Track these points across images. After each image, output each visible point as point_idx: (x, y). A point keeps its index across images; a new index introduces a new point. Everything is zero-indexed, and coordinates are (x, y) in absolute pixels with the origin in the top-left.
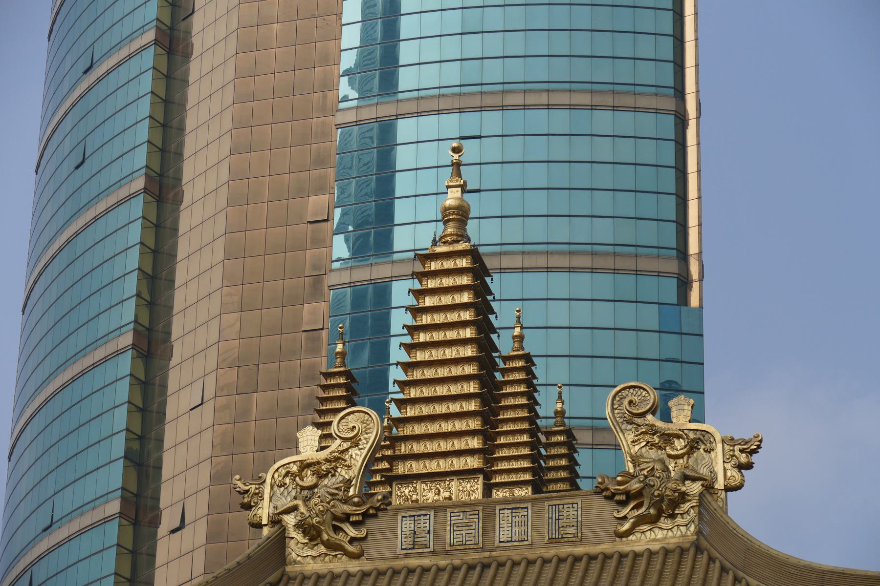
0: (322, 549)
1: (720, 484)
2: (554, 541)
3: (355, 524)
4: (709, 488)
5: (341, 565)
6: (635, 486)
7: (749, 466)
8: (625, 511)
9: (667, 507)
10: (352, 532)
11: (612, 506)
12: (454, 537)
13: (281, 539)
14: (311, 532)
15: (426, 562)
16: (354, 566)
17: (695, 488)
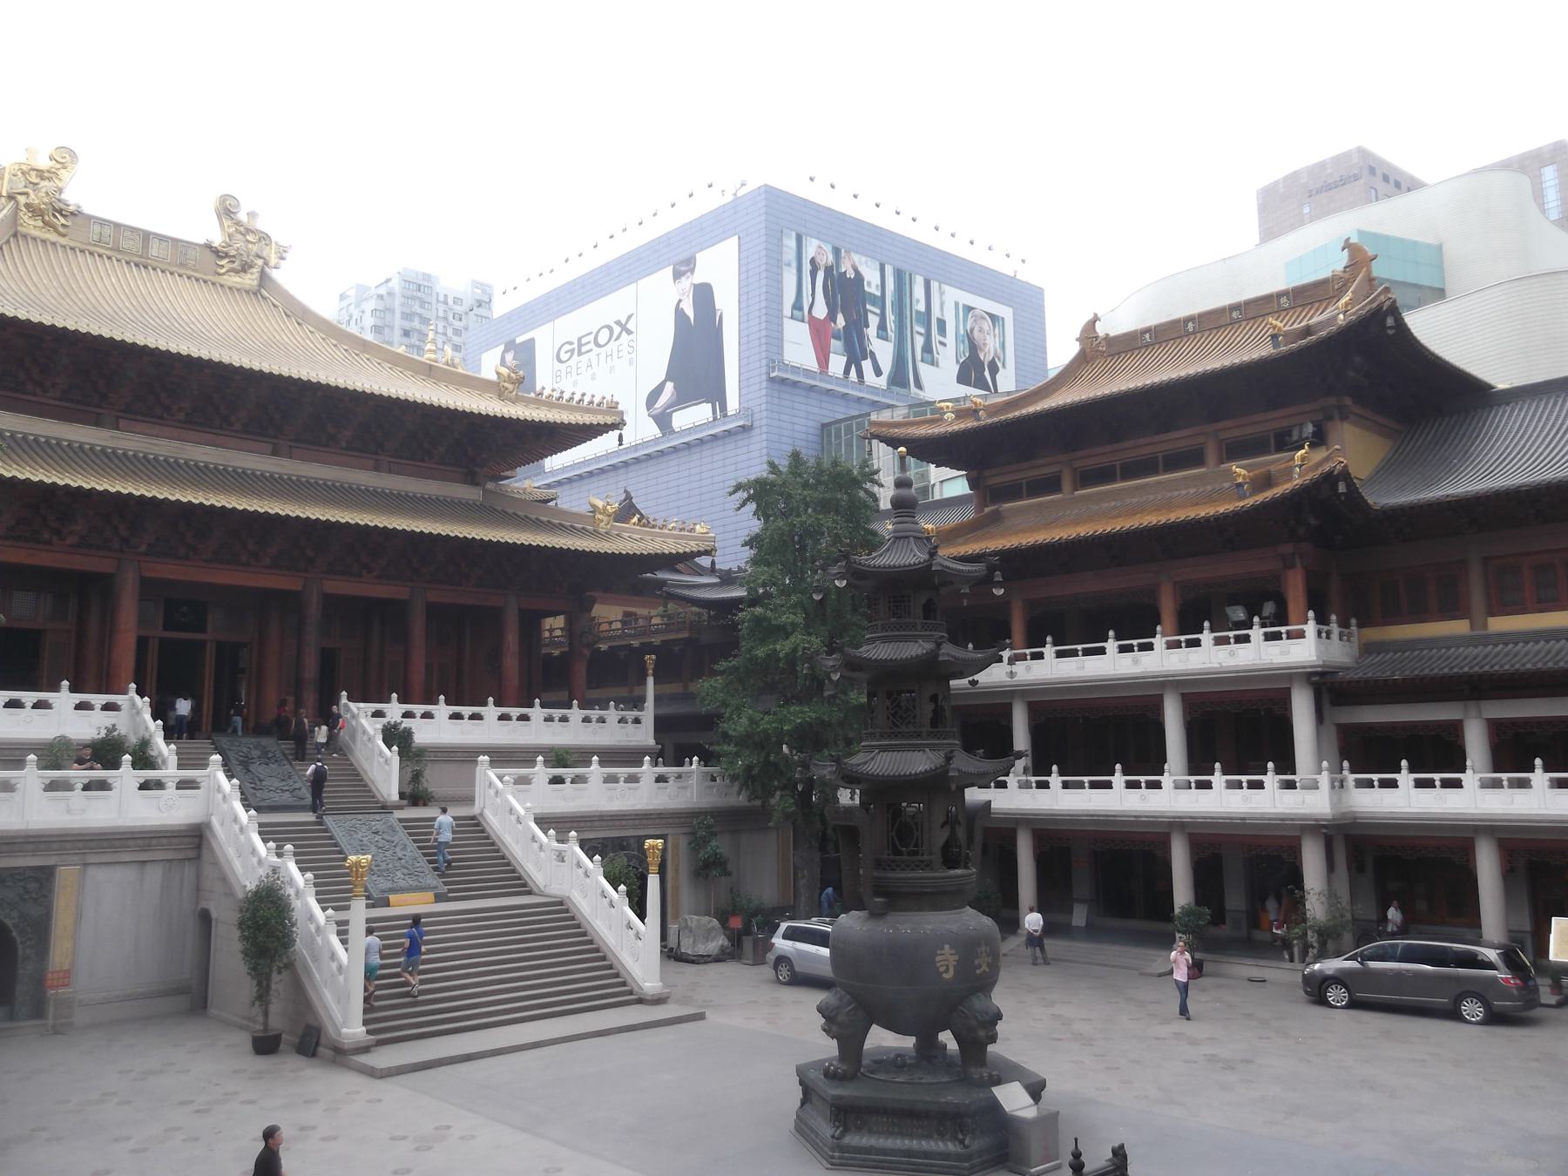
0: (40, 223)
1: (272, 263)
2: (183, 265)
3: (64, 216)
4: (266, 263)
5: (53, 237)
6: (233, 253)
7: (282, 258)
8: (223, 262)
9: (245, 268)
10: (63, 221)
11: (213, 256)
12: (124, 244)
13: (17, 208)
14: (34, 211)
15: (109, 253)
16: (63, 241)
17: (260, 262)
